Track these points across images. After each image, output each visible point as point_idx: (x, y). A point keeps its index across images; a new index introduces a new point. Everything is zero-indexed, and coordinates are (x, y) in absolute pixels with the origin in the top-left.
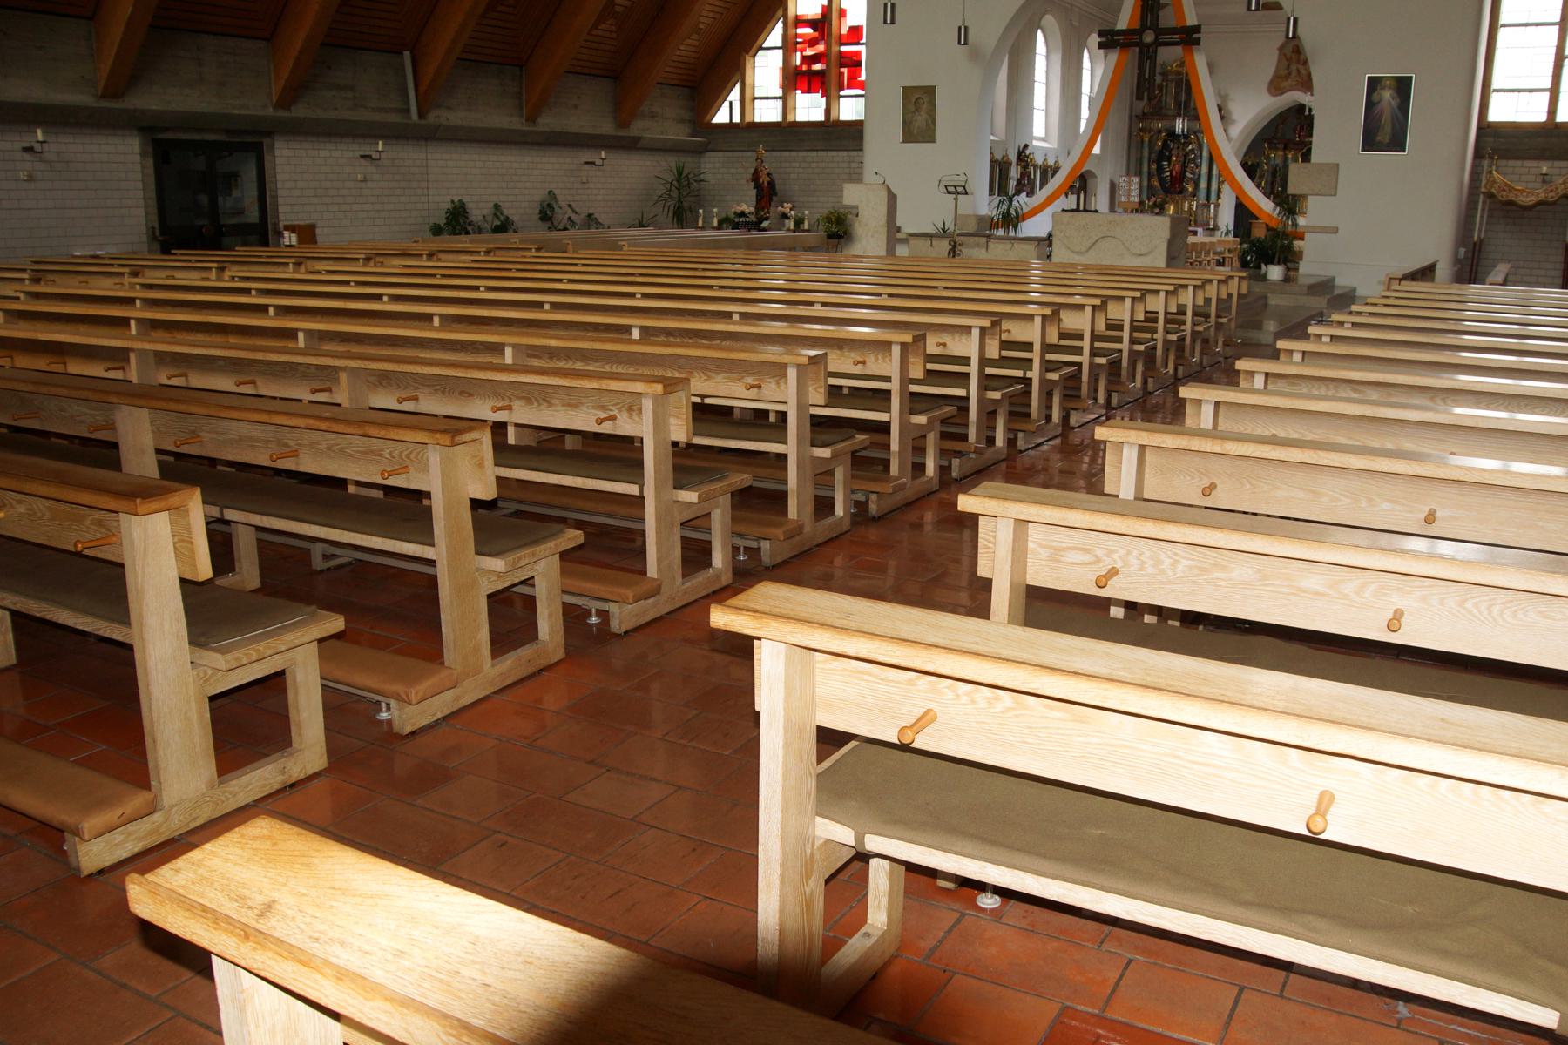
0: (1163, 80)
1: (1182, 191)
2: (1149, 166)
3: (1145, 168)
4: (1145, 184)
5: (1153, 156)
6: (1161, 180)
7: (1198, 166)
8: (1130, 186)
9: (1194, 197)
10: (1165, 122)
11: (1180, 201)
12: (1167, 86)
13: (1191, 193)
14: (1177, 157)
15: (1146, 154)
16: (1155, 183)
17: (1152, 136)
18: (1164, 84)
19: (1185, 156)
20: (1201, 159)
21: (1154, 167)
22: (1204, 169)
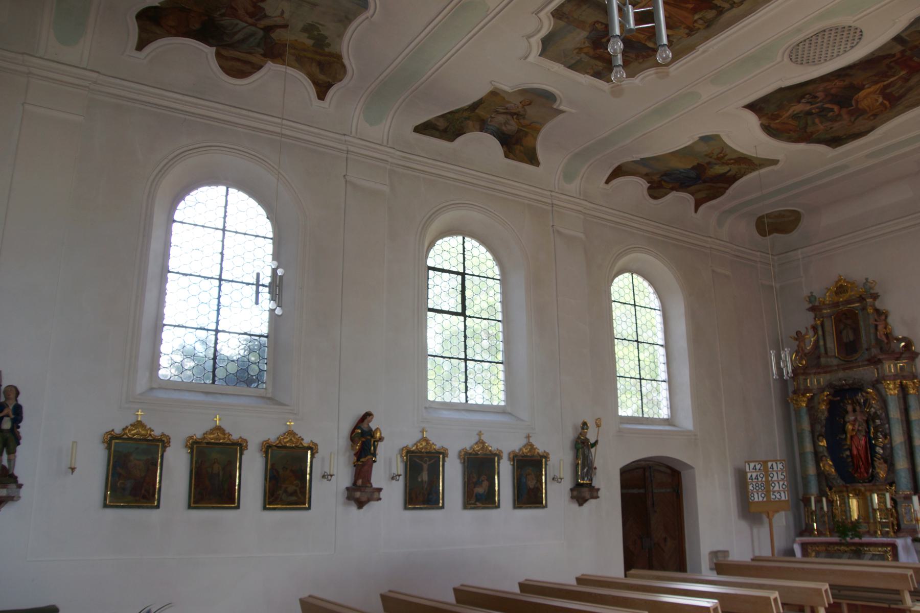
0: (815, 319)
1: (873, 478)
2: (815, 445)
3: (809, 447)
4: (812, 470)
5: (818, 428)
6: (839, 464)
7: (887, 435)
8: (767, 474)
9: (891, 485)
10: (828, 376)
11: (868, 494)
12: (822, 325)
13: (886, 479)
14: (854, 425)
15: (806, 425)
16: (828, 466)
17: (811, 400)
18: (818, 322)
19: (867, 422)
20: (889, 423)
21: (823, 443)
22: (898, 437)
